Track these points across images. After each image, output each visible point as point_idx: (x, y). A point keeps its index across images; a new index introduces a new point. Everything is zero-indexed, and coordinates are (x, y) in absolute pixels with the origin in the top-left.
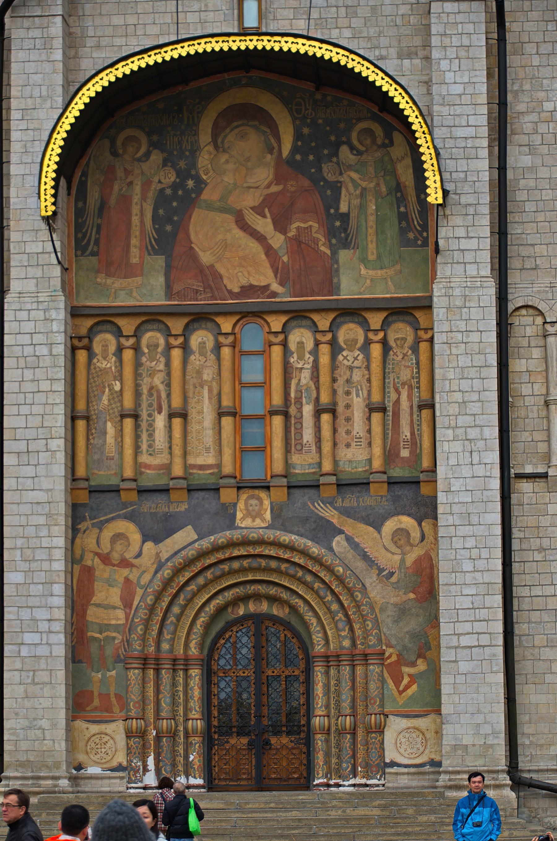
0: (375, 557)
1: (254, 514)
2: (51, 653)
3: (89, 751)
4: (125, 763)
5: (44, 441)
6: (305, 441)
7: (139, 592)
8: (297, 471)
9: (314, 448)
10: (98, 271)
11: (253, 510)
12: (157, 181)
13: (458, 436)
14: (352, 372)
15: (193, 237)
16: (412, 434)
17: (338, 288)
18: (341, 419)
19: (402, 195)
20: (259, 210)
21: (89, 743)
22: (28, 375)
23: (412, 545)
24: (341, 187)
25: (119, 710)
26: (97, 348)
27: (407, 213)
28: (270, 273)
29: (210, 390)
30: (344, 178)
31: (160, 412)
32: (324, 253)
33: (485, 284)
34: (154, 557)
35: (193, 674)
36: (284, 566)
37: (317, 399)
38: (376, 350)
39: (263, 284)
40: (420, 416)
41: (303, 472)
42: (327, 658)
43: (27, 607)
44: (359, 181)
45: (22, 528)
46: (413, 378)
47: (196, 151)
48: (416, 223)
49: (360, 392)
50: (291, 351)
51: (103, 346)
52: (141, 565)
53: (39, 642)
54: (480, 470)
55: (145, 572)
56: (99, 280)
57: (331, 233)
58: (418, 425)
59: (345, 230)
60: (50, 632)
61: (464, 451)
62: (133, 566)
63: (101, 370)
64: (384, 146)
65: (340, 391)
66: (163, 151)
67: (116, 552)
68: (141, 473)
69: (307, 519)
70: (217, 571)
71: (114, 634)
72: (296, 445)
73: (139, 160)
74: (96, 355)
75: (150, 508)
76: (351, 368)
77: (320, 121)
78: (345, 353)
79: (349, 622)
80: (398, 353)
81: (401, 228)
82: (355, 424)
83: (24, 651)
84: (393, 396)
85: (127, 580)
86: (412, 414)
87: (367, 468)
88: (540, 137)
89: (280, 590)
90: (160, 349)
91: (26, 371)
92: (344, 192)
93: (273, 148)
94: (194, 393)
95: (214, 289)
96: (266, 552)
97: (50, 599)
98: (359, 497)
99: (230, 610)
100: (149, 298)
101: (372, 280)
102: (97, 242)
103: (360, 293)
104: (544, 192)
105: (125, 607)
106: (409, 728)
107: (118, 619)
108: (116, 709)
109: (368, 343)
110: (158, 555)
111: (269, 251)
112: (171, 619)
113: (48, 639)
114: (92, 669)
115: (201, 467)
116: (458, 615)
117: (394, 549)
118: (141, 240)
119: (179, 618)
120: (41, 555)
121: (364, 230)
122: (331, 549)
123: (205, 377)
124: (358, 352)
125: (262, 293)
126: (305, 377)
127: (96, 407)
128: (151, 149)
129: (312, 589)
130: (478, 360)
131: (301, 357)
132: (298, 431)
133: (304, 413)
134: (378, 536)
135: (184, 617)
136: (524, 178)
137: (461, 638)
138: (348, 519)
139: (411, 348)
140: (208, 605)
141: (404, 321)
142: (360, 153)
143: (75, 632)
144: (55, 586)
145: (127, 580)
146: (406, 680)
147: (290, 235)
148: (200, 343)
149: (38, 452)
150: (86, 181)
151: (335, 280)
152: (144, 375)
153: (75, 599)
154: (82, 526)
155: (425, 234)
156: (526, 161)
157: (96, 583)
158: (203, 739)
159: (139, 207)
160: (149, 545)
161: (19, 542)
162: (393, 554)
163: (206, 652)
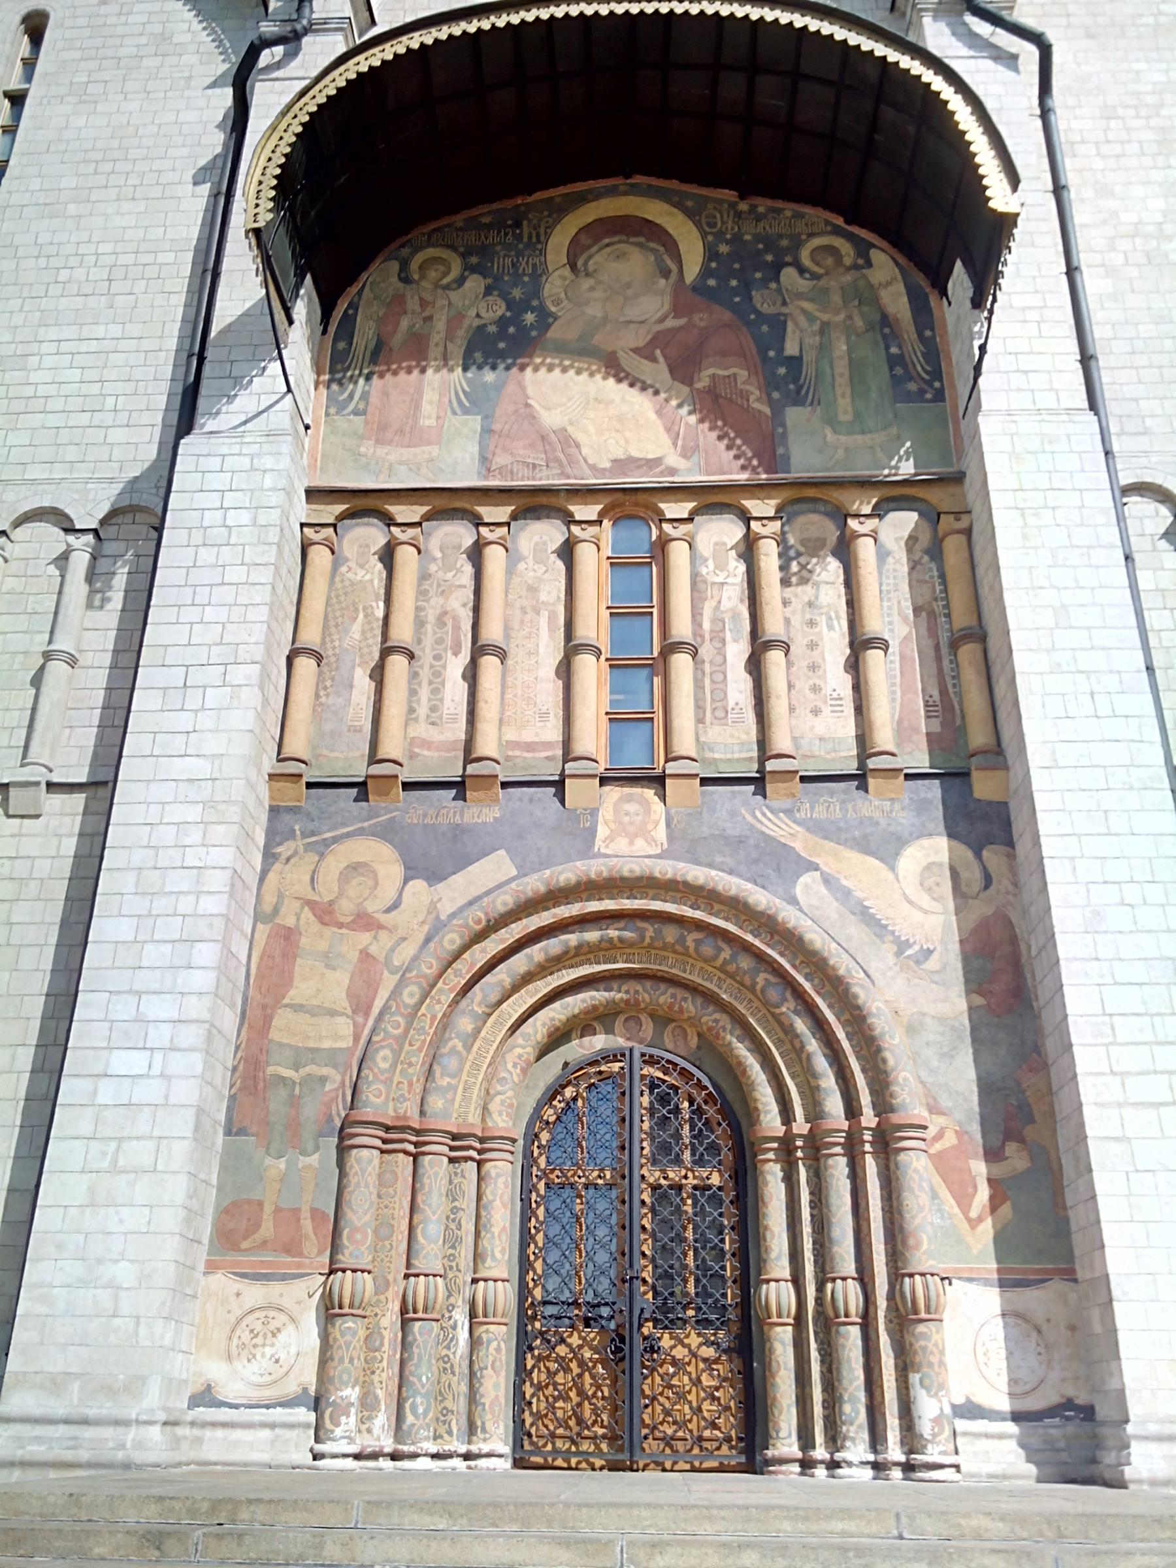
1: (631, 829)
2: (167, 1097)
3: (234, 1351)
6: (731, 703)
7: (389, 981)
8: (717, 756)
10: (362, 437)
11: (631, 823)
12: (473, 313)
13: (1059, 665)
15: (530, 391)
17: (787, 458)
18: (801, 665)
19: (892, 331)
20: (645, 352)
21: (238, 1332)
22: (207, 556)
24: (785, 322)
25: (315, 1250)
27: (902, 356)
28: (666, 441)
29: (552, 617)
31: (456, 654)
33: (1077, 418)
34: (425, 910)
35: (493, 1173)
36: (691, 938)
39: (650, 456)
40: (955, 661)
41: (729, 756)
43: (130, 992)
44: (817, 314)
45: (148, 828)
46: (936, 599)
48: (919, 368)
50: (702, 557)
52: (396, 927)
53: (144, 1071)
55: (404, 939)
56: (362, 449)
57: (770, 384)
58: (953, 677)
59: (796, 380)
62: (381, 927)
63: (352, 584)
64: (855, 267)
65: (796, 621)
67: (349, 898)
68: (412, 756)
69: (740, 841)
70: (554, 945)
71: (325, 1071)
73: (447, 287)
74: (347, 560)
75: (425, 816)
77: (748, 237)
81: (893, 376)
82: (829, 675)
83: (107, 1093)
85: (365, 955)
88: (1121, 256)
89: (681, 993)
91: (202, 550)
92: (790, 326)
93: (670, 271)
94: (522, 622)
97: (183, 975)
98: (843, 802)
101: (846, 450)
103: (828, 470)
104: (1141, 328)
105: (354, 1012)
107: (336, 1037)
110: (433, 907)
113: (164, 1065)
114: (268, 1148)
115: (531, 747)
116: (1113, 1028)
120: (179, 881)
121: (829, 379)
122: (793, 901)
123: (543, 597)
125: (651, 468)
127: (337, 643)
129: (752, 989)
131: (720, 566)
134: (891, 876)
137: (1129, 1081)
139: (927, 552)
142: (815, 277)
143: (241, 1067)
144: (199, 946)
145: (365, 955)
148: (537, 544)
149: (205, 687)
151: (780, 451)
152: (431, 593)
153: (251, 993)
154: (284, 850)
155: (937, 384)
157: (299, 961)
159: (441, 349)
160: (418, 885)
161: (137, 857)
162: (926, 912)
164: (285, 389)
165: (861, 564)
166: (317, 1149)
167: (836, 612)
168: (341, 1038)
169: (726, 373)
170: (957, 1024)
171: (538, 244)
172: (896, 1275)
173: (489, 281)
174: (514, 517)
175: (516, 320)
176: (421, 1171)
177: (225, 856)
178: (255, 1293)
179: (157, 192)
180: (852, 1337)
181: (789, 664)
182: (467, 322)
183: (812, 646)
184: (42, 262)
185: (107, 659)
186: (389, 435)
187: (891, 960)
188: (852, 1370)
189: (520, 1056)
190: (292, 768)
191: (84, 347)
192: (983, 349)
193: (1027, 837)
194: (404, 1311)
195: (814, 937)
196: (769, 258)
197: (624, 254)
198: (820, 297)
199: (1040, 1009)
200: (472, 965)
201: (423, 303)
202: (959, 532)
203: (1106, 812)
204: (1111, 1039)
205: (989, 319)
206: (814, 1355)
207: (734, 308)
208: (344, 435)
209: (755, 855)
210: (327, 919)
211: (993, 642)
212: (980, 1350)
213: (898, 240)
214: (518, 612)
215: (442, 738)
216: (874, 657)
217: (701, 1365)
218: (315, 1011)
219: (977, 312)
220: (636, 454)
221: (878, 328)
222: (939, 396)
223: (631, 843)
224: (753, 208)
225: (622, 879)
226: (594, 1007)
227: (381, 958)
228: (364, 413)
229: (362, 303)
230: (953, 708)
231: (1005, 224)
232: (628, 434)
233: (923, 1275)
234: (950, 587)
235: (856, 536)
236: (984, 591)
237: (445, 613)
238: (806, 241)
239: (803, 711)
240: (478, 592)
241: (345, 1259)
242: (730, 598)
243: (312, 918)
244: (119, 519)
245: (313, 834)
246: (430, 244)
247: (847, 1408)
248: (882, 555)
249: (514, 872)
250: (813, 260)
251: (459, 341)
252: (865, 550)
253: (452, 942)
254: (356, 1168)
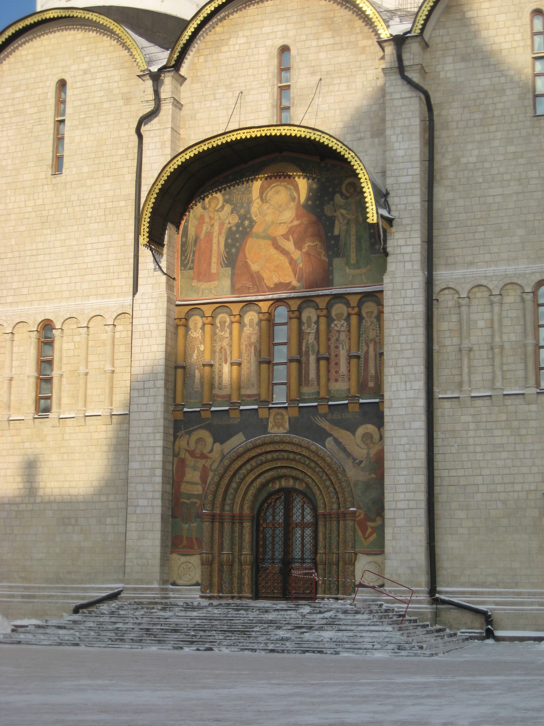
2: (153, 511)
4: (200, 582)
5: (153, 382)
6: (310, 378)
7: (211, 474)
8: (305, 397)
9: (316, 383)
10: (193, 279)
11: (278, 422)
12: (227, 222)
14: (339, 334)
15: (247, 256)
16: (376, 372)
18: (333, 364)
20: (285, 237)
22: (146, 341)
23: (374, 443)
26: (191, 324)
28: (292, 275)
30: (337, 214)
31: (226, 363)
35: (246, 526)
36: (298, 457)
37: (318, 352)
38: (354, 320)
39: (287, 282)
42: (324, 515)
47: (250, 203)
54: (411, 394)
55: (214, 461)
56: (193, 284)
60: (153, 498)
61: (401, 382)
62: (207, 458)
65: (332, 347)
66: (231, 204)
72: (305, 381)
73: (218, 211)
74: (191, 329)
76: (339, 332)
78: (335, 322)
79: (336, 493)
80: (368, 321)
83: (138, 511)
84: (365, 348)
86: (376, 360)
87: (348, 394)
89: (298, 472)
90: (227, 324)
92: (337, 222)
96: (286, 449)
99: (270, 485)
101: (353, 276)
102: (193, 261)
104: (460, 215)
106: (371, 562)
108: (196, 547)
109: (349, 315)
110: (222, 451)
111: (292, 262)
112: (231, 491)
117: (362, 445)
118: (218, 259)
119: (236, 490)
122: (325, 446)
124: (344, 322)
126: (311, 339)
130: (411, 322)
131: (309, 326)
133: (311, 361)
135: (239, 490)
136: (448, 207)
139: (375, 318)
140: (255, 482)
141: (372, 301)
142: (347, 198)
146: (369, 530)
147: (304, 250)
148: (250, 320)
150: (188, 225)
151: (331, 277)
152: (218, 340)
154: (179, 434)
156: (449, 195)
158: (252, 567)
159: (217, 239)
160: (217, 445)
161: (138, 444)
162: (362, 448)
163: (255, 512)
177: (160, 443)
183: (337, 356)
201: (211, 218)
223: (278, 429)
227: (209, 467)
239: (332, 380)
249: (245, 439)
250: (347, 190)
253: (227, 463)
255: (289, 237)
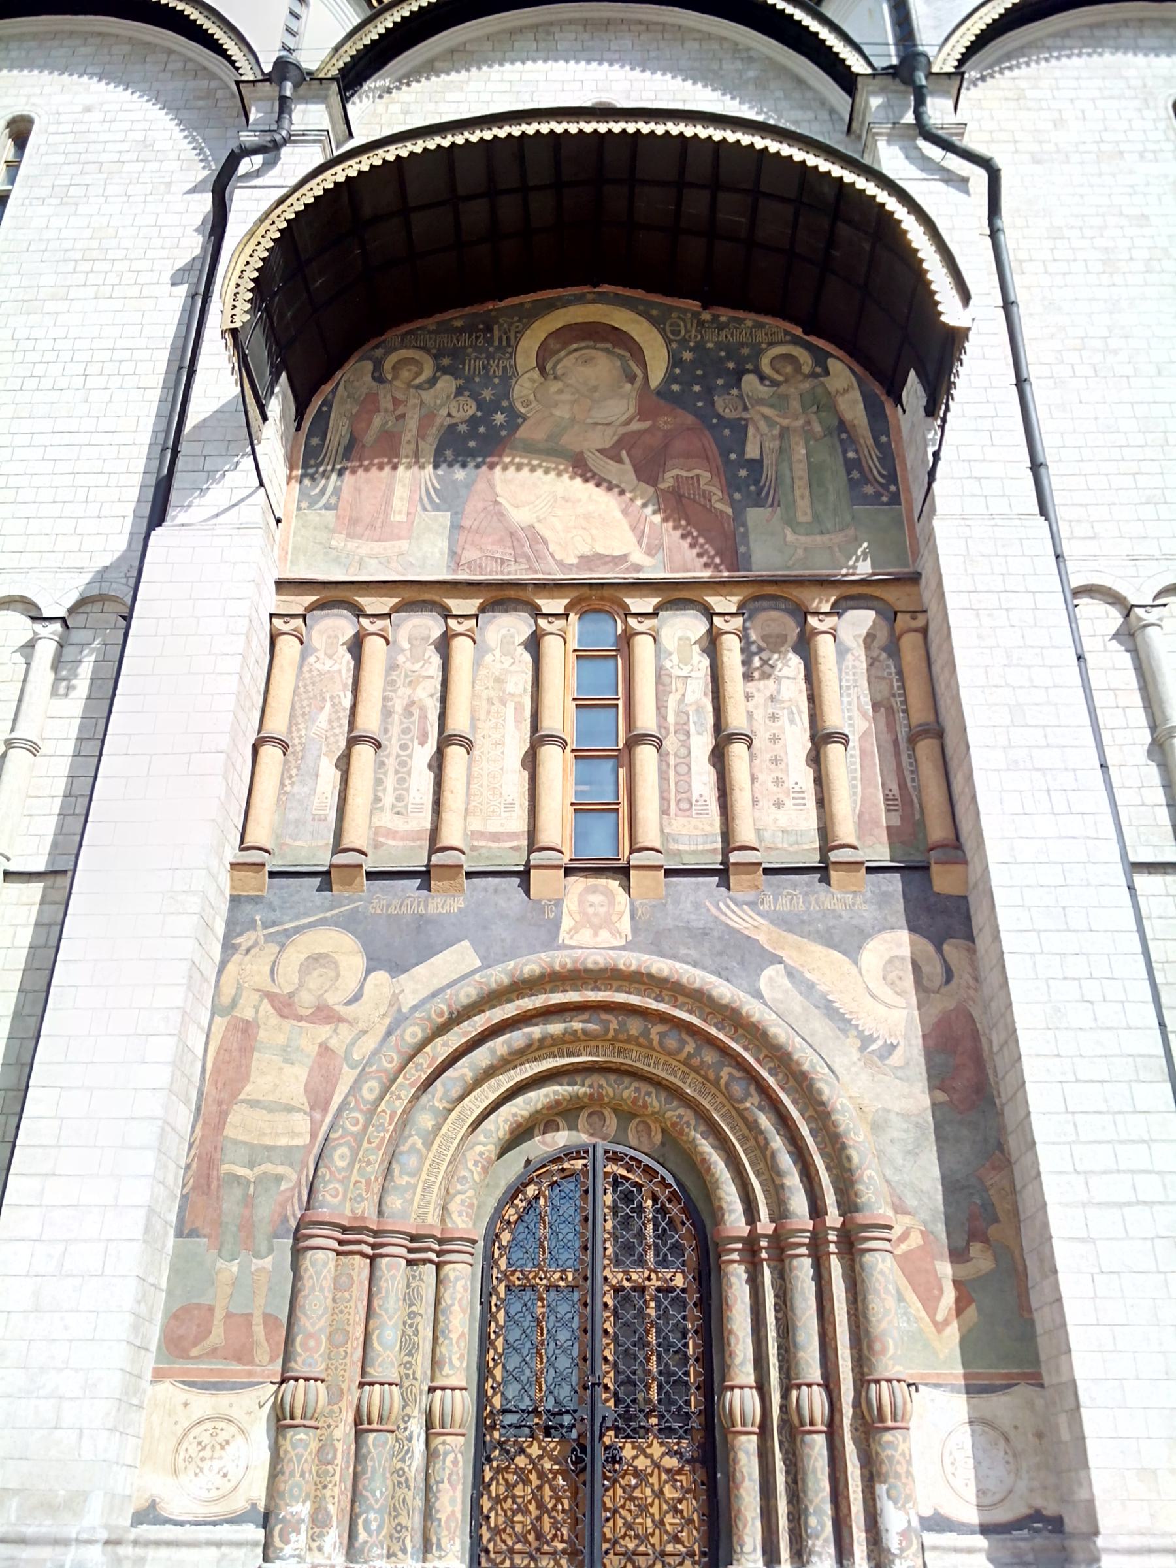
0: (851, 1013)
6: (695, 797)
8: (681, 847)
10: (333, 531)
11: (596, 915)
12: (445, 413)
13: (1016, 762)
14: (780, 684)
15: (498, 489)
17: (748, 556)
19: (849, 437)
20: (612, 454)
24: (746, 426)
25: (267, 1358)
27: (859, 460)
28: (631, 538)
29: (518, 708)
31: (422, 744)
32: (722, 512)
34: (387, 1003)
35: (452, 1276)
36: (655, 1031)
39: (616, 553)
41: (693, 848)
44: (777, 419)
46: (894, 695)
47: (511, 378)
49: (797, 717)
50: (666, 651)
51: (329, 637)
52: (356, 1020)
55: (365, 1032)
57: (732, 485)
58: (912, 772)
59: (757, 482)
62: (341, 1020)
63: (320, 673)
64: (814, 375)
65: (759, 715)
67: (309, 990)
68: (377, 846)
69: (705, 933)
71: (281, 1170)
73: (419, 387)
74: (316, 650)
75: (388, 906)
77: (710, 345)
81: (850, 480)
85: (325, 1049)
89: (645, 1087)
92: (751, 430)
93: (635, 376)
94: (488, 713)
95: (533, 558)
98: (806, 894)
100: (419, 570)
101: (805, 549)
103: (788, 568)
107: (293, 1134)
110: (394, 999)
114: (220, 1250)
115: (495, 837)
116: (1075, 1125)
121: (788, 481)
122: (758, 995)
123: (510, 688)
125: (616, 565)
127: (303, 733)
128: (438, 374)
131: (685, 660)
132: (685, 778)
134: (854, 970)
138: (790, 935)
139: (884, 649)
142: (775, 384)
143: (194, 1165)
145: (325, 1049)
147: (662, 486)
148: (504, 637)
151: (742, 549)
153: (206, 1089)
154: (244, 941)
159: (413, 446)
162: (889, 1006)
164: (258, 484)
165: (821, 660)
166: (270, 1250)
167: (797, 706)
168: (299, 1135)
169: (690, 474)
170: (921, 1121)
171: (508, 347)
172: (862, 1381)
173: (461, 382)
174: (483, 609)
175: (486, 419)
176: (378, 1273)
178: (203, 1403)
179: (135, 291)
180: (818, 1446)
181: (752, 757)
182: (438, 421)
183: (774, 739)
184: (19, 357)
185: (69, 747)
186: (359, 529)
187: (855, 1055)
188: (817, 1481)
189: (481, 1154)
190: (255, 857)
191: (57, 440)
192: (936, 455)
193: (987, 930)
194: (358, 1421)
195: (779, 1032)
196: (731, 365)
197: (592, 359)
198: (780, 402)
199: (1003, 1105)
200: (434, 1059)
201: (396, 402)
202: (916, 630)
203: (1064, 908)
204: (1074, 1138)
205: (942, 427)
206: (779, 1465)
207: (697, 413)
208: (315, 528)
209: (719, 947)
210: (286, 1011)
211: (951, 740)
212: (948, 1460)
213: (855, 351)
214: (484, 704)
215: (407, 827)
216: (834, 751)
217: (664, 1477)
218: (274, 1108)
219: (930, 420)
220: (601, 550)
221: (835, 433)
222: (895, 499)
223: (596, 934)
224: (715, 317)
225: (587, 971)
226: (558, 1102)
227: (341, 1053)
228: (335, 508)
229: (336, 400)
230: (912, 801)
231: (954, 339)
232: (594, 531)
233: (889, 1381)
234: (907, 686)
235: (815, 633)
236: (941, 688)
237: (413, 703)
238: (767, 350)
240: (445, 683)
241: (299, 1367)
242: (694, 692)
243: (272, 1011)
244: (88, 608)
245: (274, 924)
246: (403, 345)
247: (813, 1521)
248: (842, 652)
249: (478, 963)
250: (773, 368)
251: (430, 439)
252: (825, 646)
253: (414, 1035)
254: (311, 1270)
255: (619, 454)
